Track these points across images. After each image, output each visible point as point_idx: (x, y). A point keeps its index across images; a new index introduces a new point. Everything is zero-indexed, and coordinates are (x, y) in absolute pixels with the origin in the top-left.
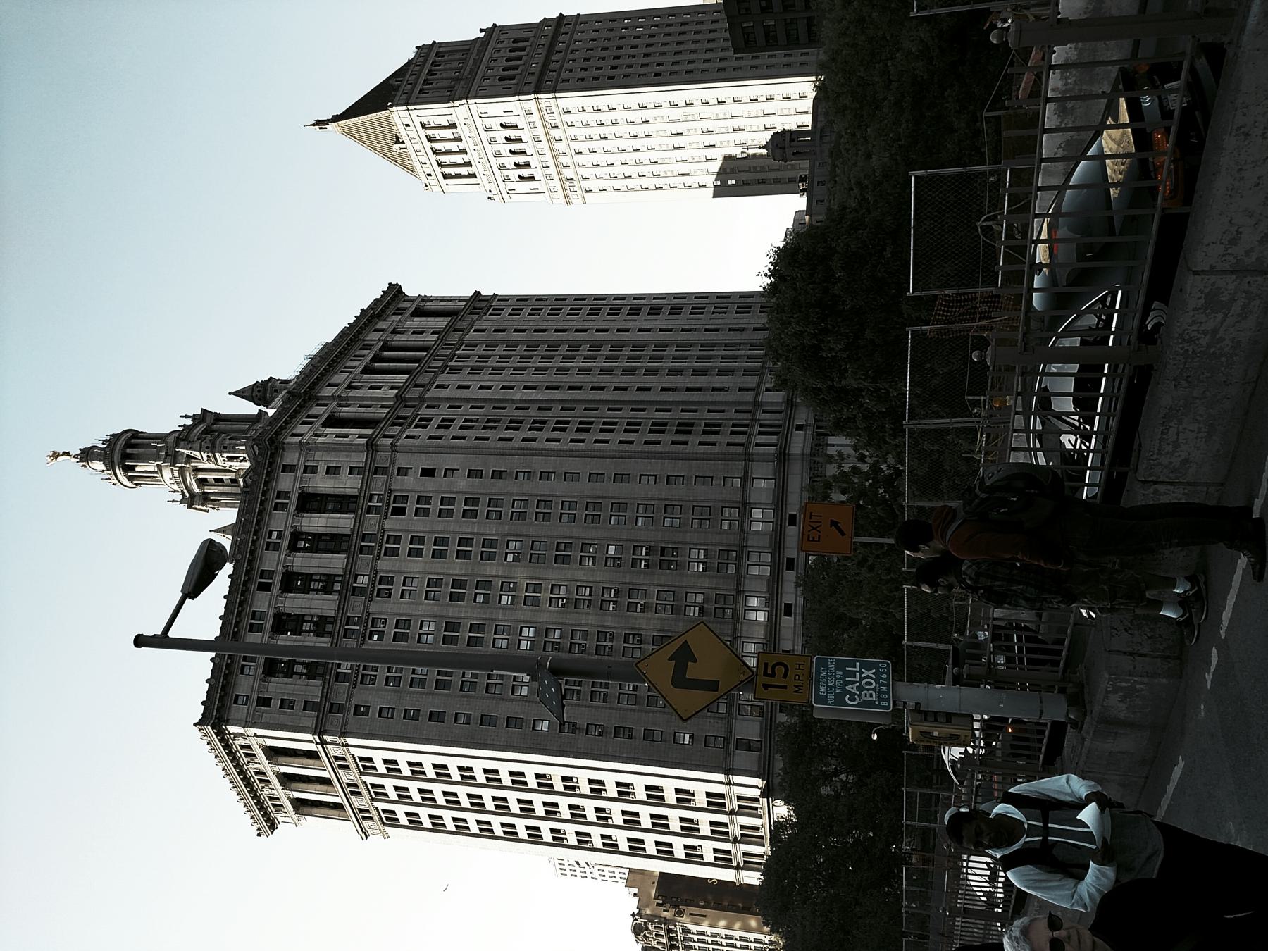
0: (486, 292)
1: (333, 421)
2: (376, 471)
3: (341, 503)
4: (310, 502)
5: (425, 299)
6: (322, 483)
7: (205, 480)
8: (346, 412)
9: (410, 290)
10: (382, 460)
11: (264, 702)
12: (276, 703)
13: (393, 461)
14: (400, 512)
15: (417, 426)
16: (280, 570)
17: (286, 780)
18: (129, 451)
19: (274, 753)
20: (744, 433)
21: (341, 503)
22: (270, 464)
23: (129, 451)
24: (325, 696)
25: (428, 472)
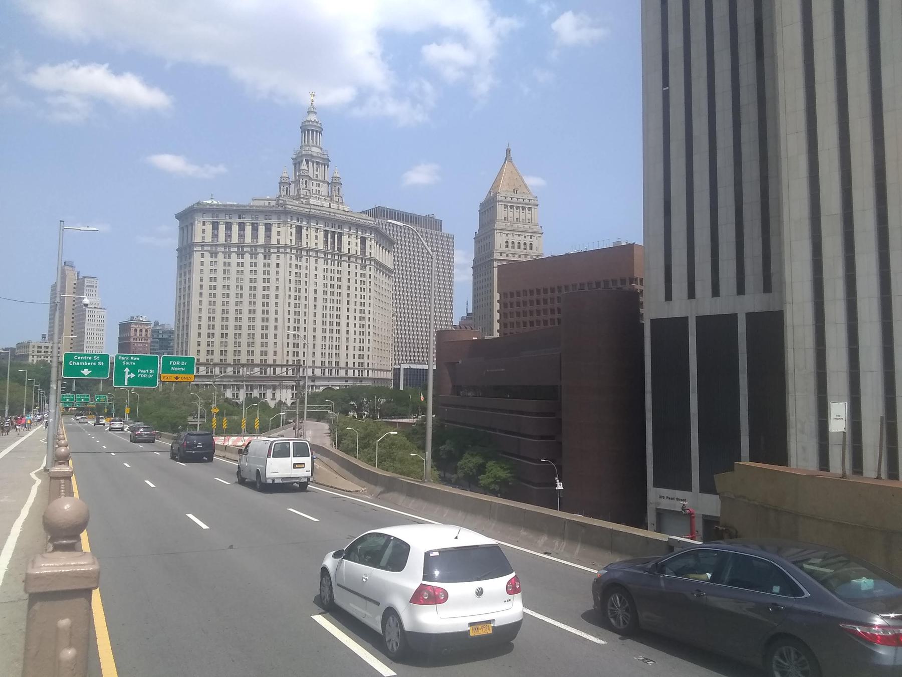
1: (299, 229)
3: (268, 237)
4: (268, 228)
6: (274, 229)
8: (304, 232)
11: (204, 224)
14: (265, 258)
21: (268, 237)
25: (278, 265)
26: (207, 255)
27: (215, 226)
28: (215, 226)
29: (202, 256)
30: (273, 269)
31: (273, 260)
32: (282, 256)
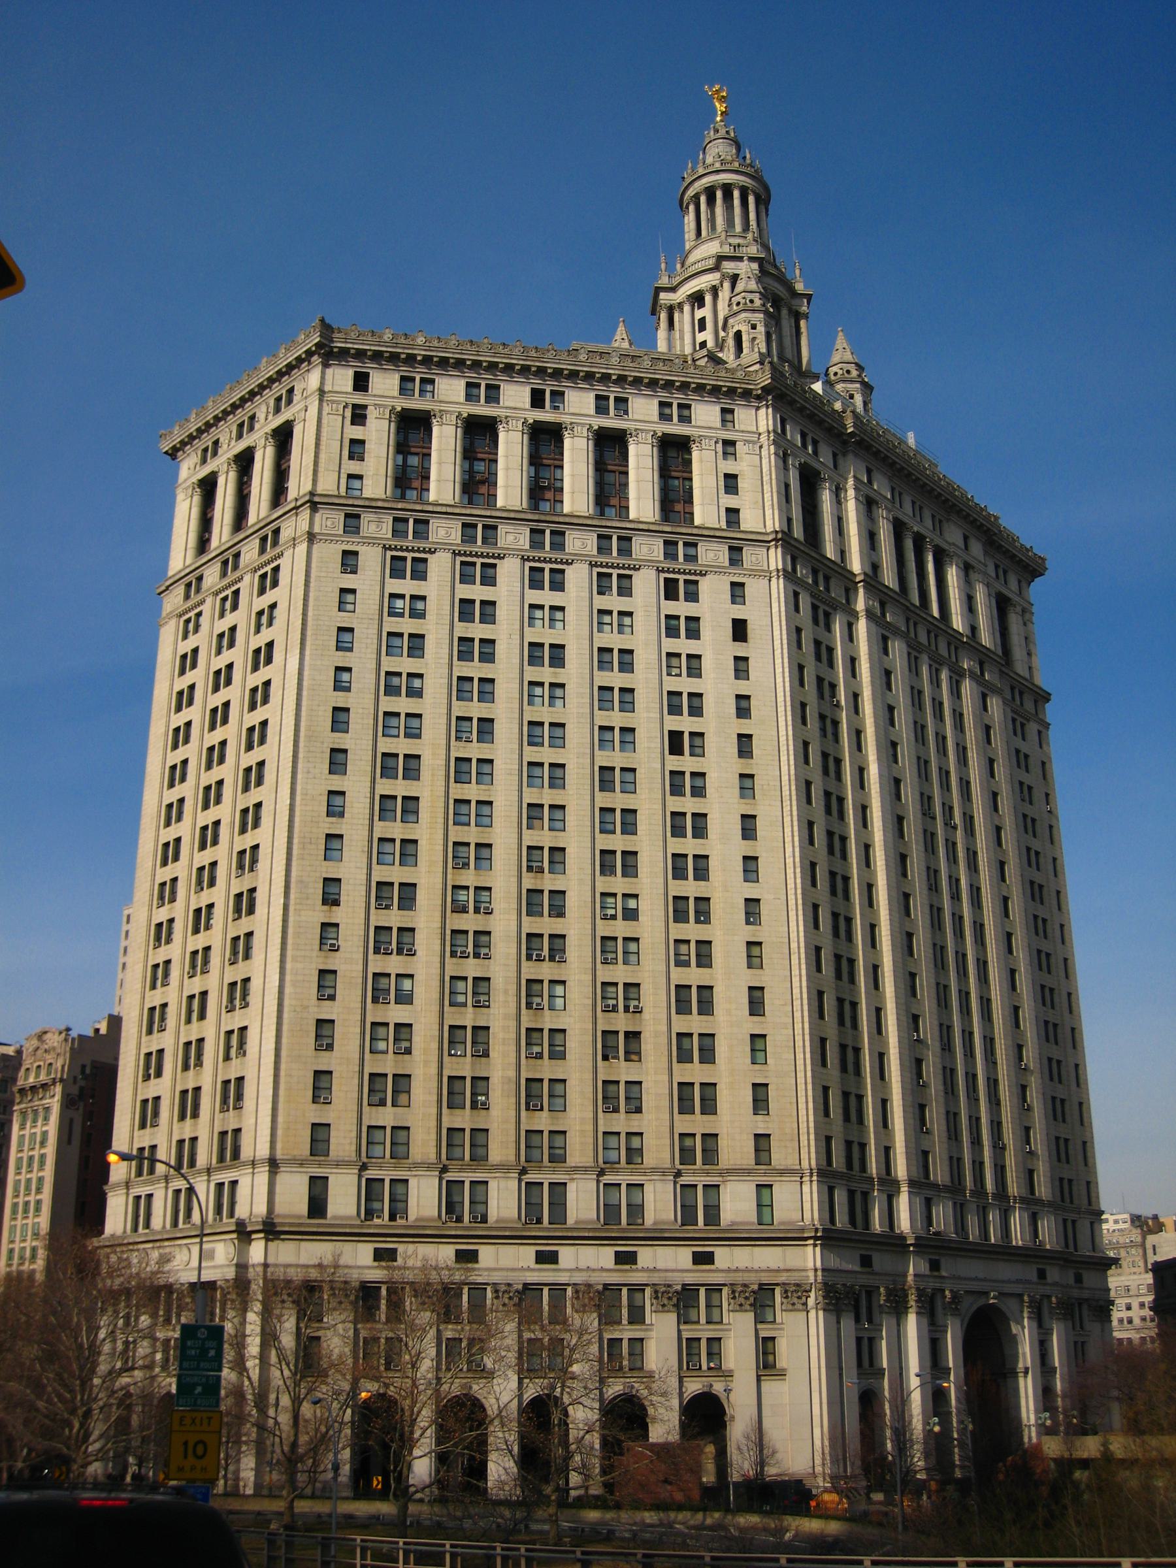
0: (1051, 711)
2: (735, 552)
3: (674, 497)
4: (674, 452)
5: (1026, 611)
7: (702, 305)
9: (1037, 589)
10: (750, 556)
11: (359, 416)
12: (356, 432)
13: (756, 573)
14: (670, 591)
15: (815, 608)
16: (566, 419)
17: (244, 462)
18: (736, 194)
19: (283, 437)
20: (849, 1165)
21: (674, 497)
22: (731, 392)
23: (736, 194)
24: (372, 506)
25: (740, 630)
26: (371, 559)
27: (412, 428)
28: (412, 428)
29: (349, 561)
30: (713, 644)
31: (713, 605)
32: (754, 588)
